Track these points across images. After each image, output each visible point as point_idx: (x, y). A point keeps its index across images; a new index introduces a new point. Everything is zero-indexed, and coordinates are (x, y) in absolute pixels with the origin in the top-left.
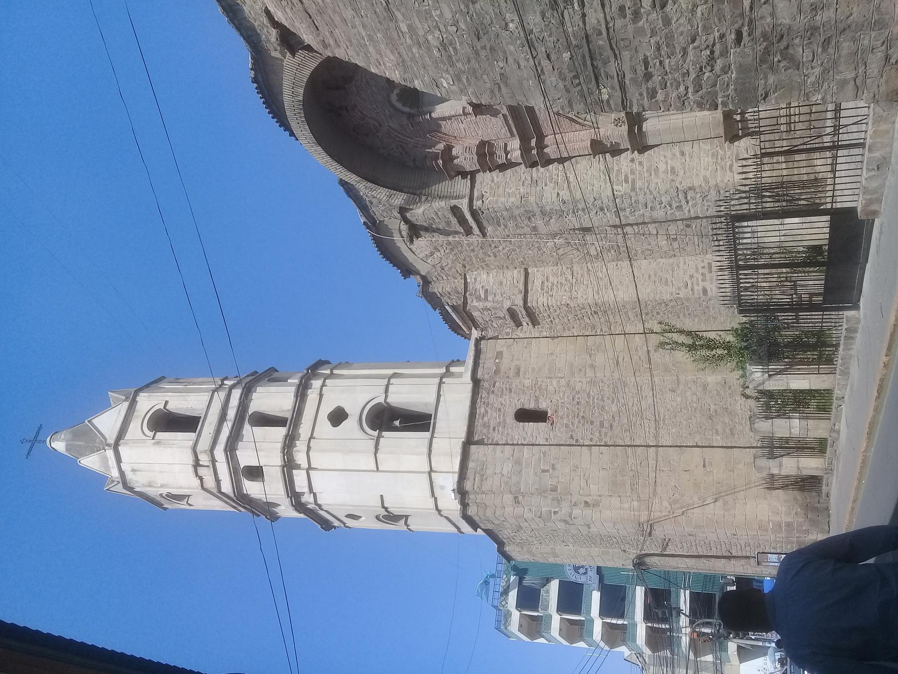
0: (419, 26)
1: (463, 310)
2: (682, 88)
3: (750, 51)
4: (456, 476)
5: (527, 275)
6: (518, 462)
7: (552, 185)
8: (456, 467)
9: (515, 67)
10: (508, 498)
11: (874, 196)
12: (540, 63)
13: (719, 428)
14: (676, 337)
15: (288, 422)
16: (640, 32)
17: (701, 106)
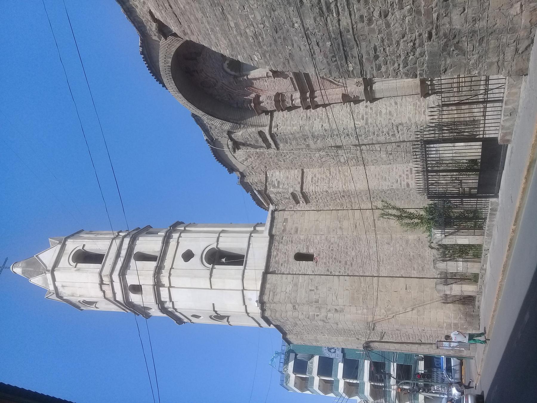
0: (242, 24)
1: (264, 193)
2: (396, 65)
3: (436, 44)
4: (259, 292)
6: (296, 285)
7: (319, 120)
8: (259, 287)
9: (298, 49)
10: (289, 306)
11: (508, 131)
12: (312, 48)
13: (415, 266)
14: (391, 211)
15: (158, 259)
16: (372, 31)
17: (407, 75)
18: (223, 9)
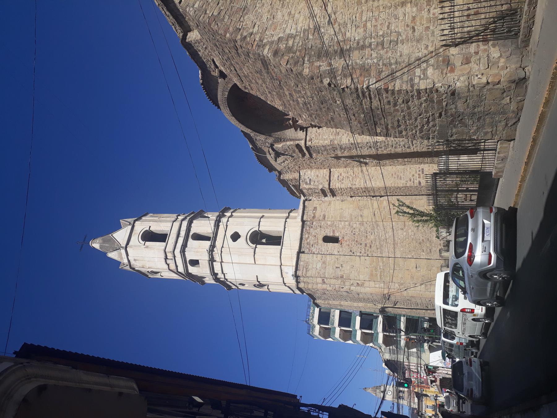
1: (298, 187)
2: (414, 131)
4: (294, 268)
5: (330, 172)
6: (324, 263)
8: (294, 263)
10: (319, 280)
16: (397, 110)
18: (280, 83)
